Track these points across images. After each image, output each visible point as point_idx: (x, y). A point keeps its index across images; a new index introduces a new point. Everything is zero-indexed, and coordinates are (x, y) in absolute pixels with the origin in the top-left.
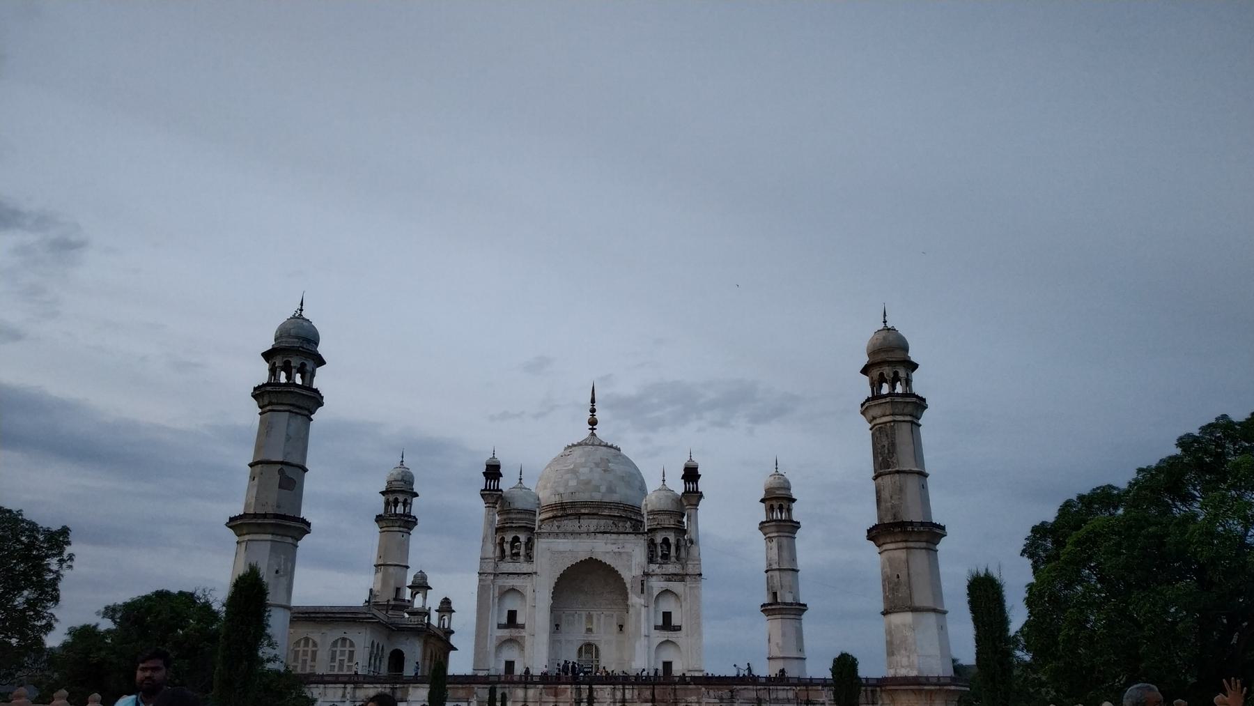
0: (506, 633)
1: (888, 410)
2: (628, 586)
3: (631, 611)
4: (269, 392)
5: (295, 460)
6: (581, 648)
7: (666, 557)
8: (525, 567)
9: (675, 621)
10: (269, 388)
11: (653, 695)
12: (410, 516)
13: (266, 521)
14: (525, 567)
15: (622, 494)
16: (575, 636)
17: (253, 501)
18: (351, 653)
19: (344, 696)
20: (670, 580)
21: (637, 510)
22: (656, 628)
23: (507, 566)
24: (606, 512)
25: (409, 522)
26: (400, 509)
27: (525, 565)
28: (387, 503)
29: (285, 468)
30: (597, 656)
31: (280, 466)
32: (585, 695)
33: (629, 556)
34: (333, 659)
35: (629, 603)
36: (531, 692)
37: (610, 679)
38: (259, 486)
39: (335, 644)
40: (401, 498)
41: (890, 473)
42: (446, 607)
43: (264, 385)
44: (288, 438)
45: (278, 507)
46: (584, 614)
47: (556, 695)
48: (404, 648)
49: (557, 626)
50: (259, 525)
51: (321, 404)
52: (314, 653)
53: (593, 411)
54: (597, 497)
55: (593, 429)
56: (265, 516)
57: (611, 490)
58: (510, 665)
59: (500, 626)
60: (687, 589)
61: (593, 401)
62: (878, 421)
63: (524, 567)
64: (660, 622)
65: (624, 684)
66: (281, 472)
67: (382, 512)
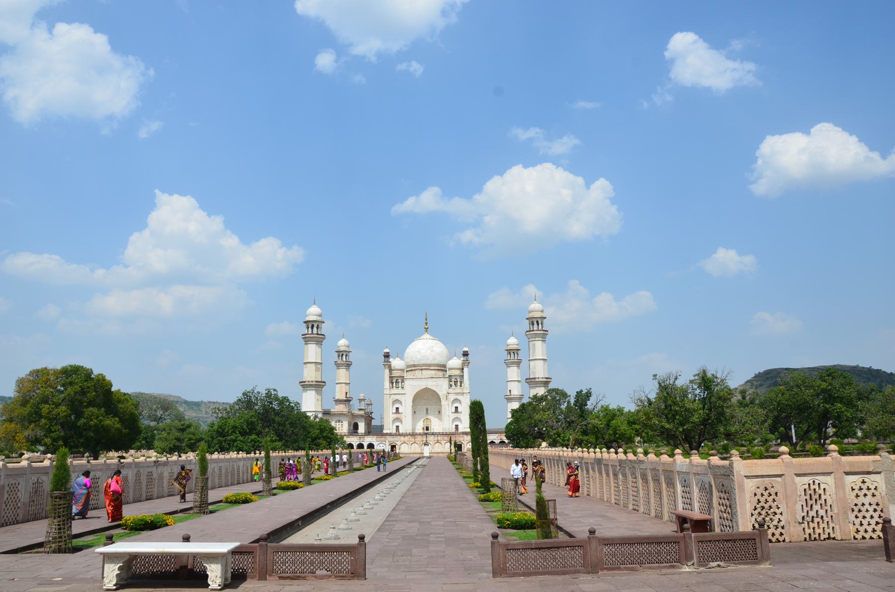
0: (396, 416)
7: (456, 382)
8: (402, 391)
9: (459, 410)
14: (402, 391)
21: (445, 366)
23: (395, 391)
32: (425, 439)
33: (441, 386)
36: (406, 438)
37: (433, 434)
46: (425, 407)
54: (429, 362)
57: (434, 359)
58: (397, 427)
63: (400, 391)
64: (454, 410)
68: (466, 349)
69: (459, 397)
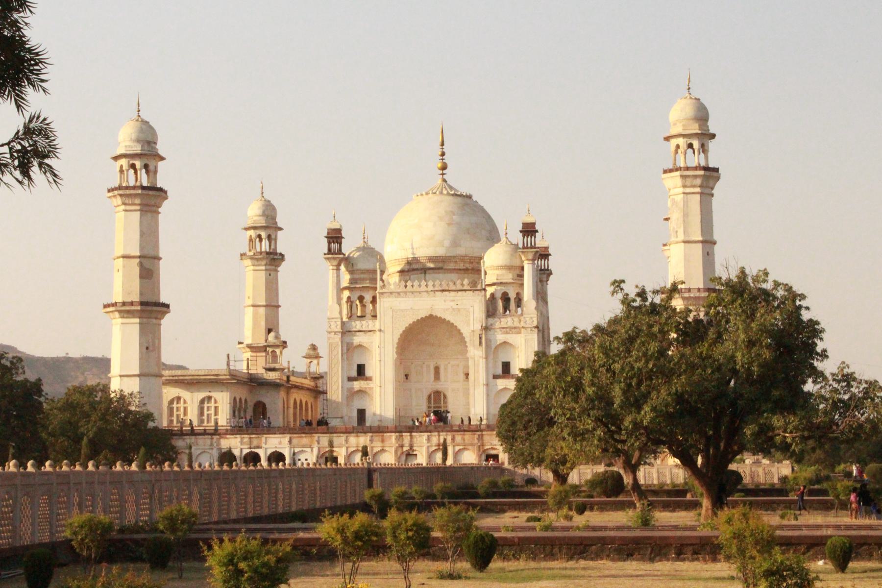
0: (357, 385)
1: (679, 181)
2: (467, 340)
3: (471, 363)
4: (121, 195)
5: (151, 253)
6: (430, 396)
10: (121, 192)
11: (464, 440)
12: (276, 254)
13: (133, 308)
15: (467, 248)
16: (427, 385)
17: (121, 289)
18: (216, 408)
19: (212, 444)
20: (507, 333)
22: (495, 377)
24: (452, 266)
25: (274, 259)
26: (265, 246)
27: (370, 322)
28: (251, 240)
29: (143, 260)
30: (445, 403)
31: (138, 260)
34: (201, 413)
35: (468, 355)
38: (124, 276)
39: (202, 402)
40: (264, 234)
41: (677, 242)
42: (313, 353)
43: (115, 189)
44: (142, 234)
45: (141, 294)
47: (383, 441)
48: (266, 400)
49: (407, 376)
50: (128, 312)
51: (166, 198)
52: (185, 409)
53: (443, 154)
54: (441, 252)
55: (443, 174)
56: (132, 304)
57: (455, 243)
59: (350, 379)
60: (523, 342)
61: (443, 144)
62: (672, 192)
65: (439, 432)
66: (141, 265)
67: (245, 249)
68: (529, 220)
69: (510, 338)
